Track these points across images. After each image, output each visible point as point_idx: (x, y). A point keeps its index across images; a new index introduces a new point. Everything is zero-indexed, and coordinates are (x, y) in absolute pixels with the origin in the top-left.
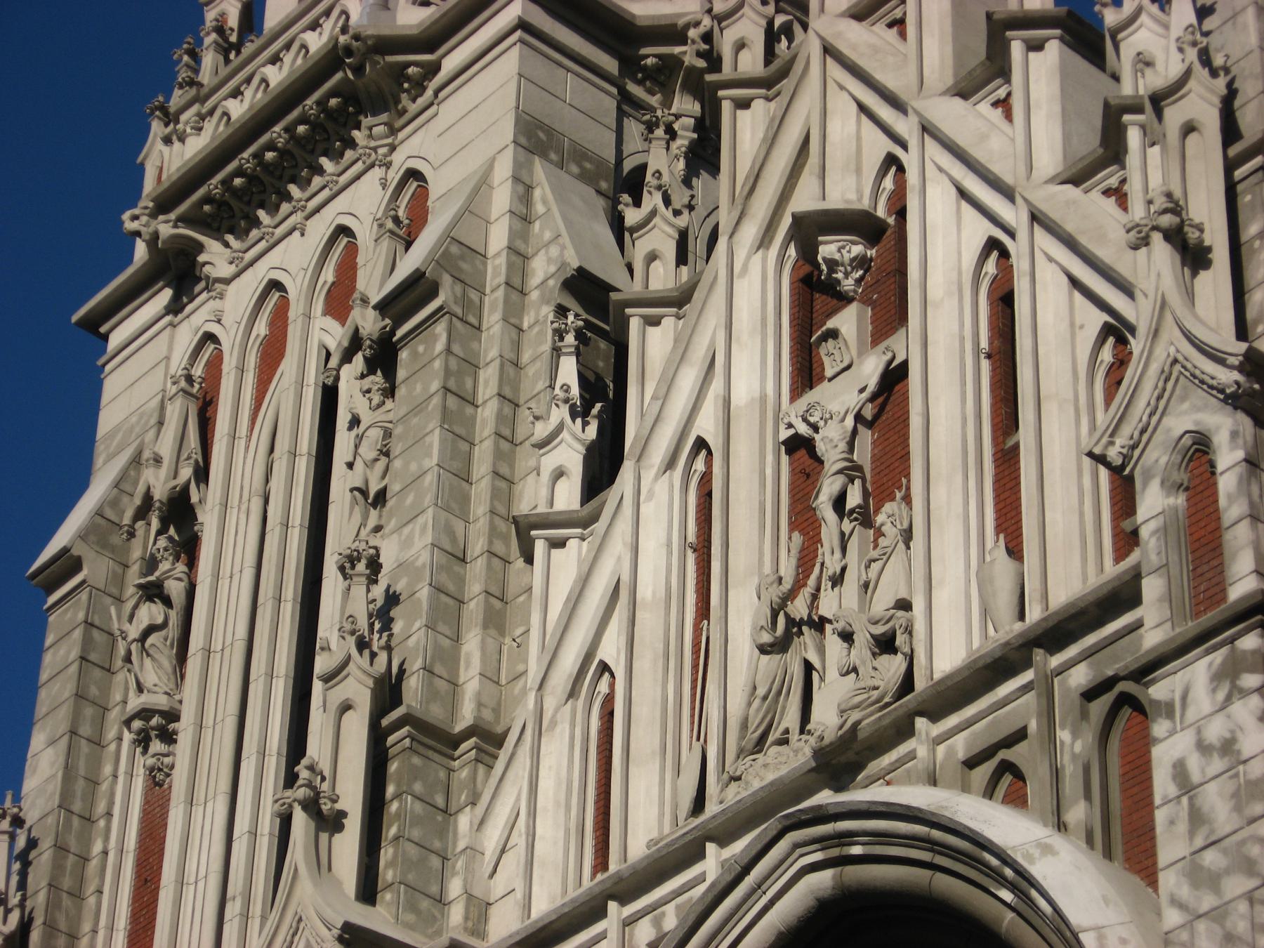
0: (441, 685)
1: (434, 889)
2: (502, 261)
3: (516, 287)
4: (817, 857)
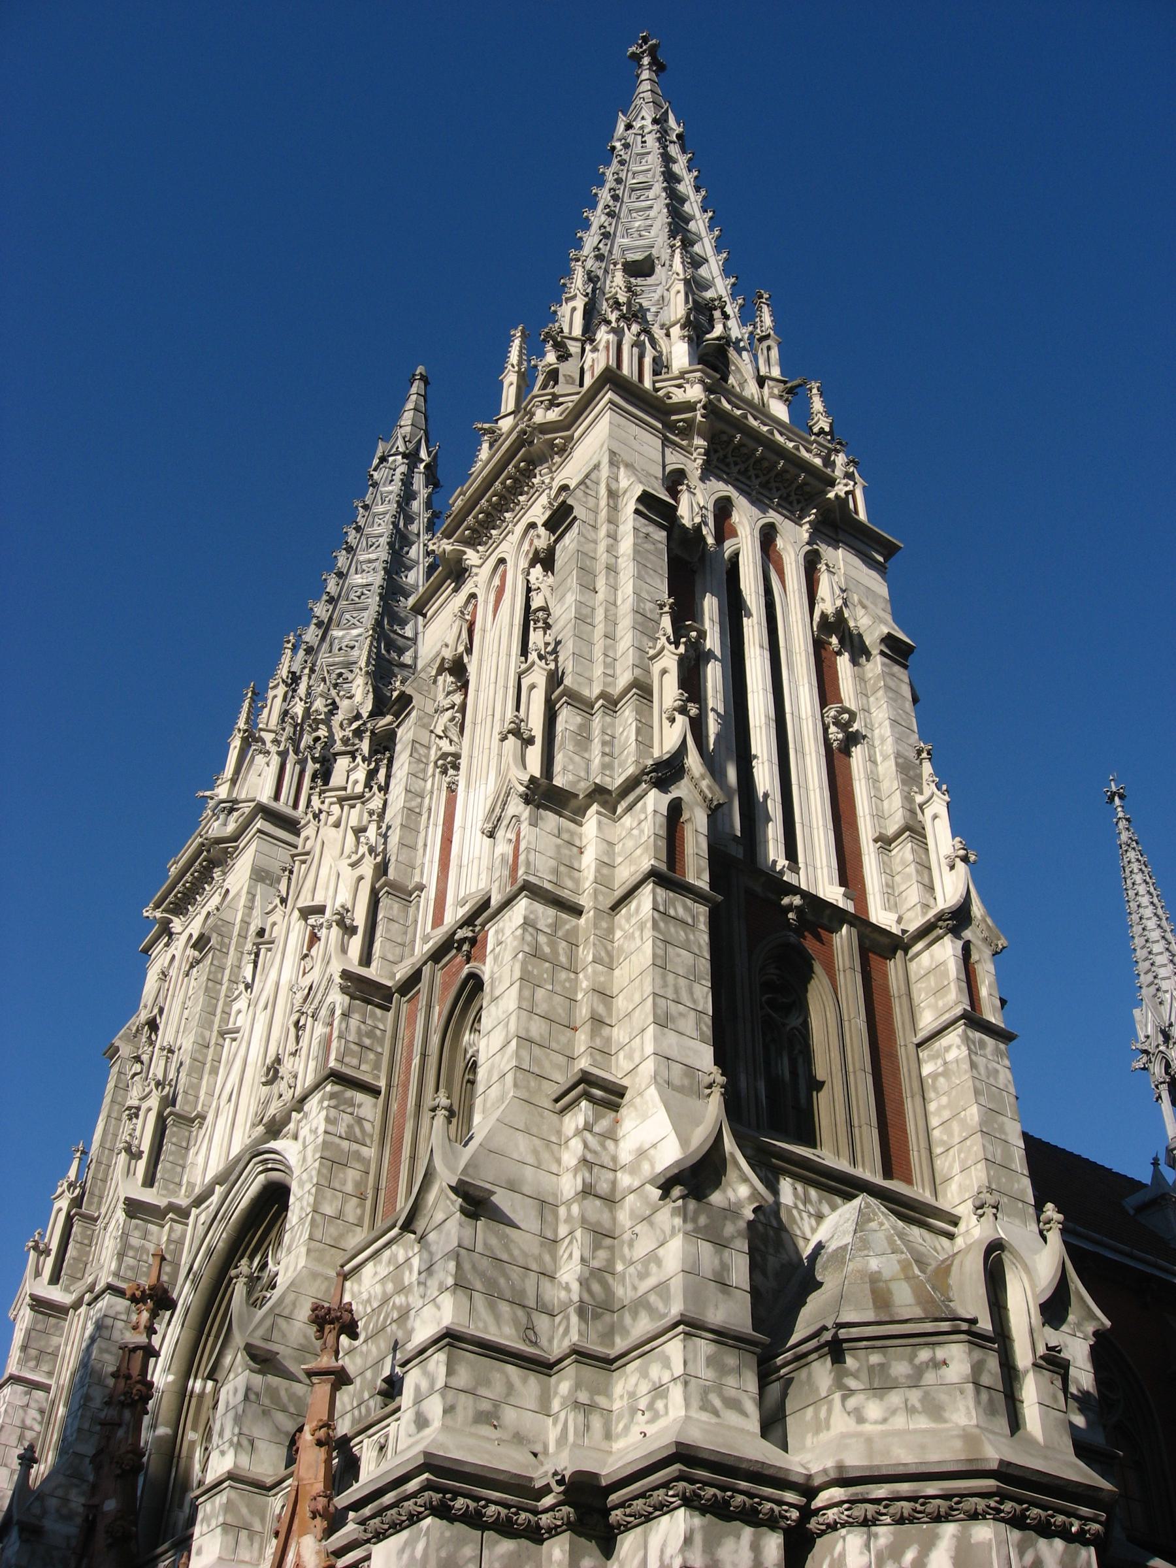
0: (191, 1098)
4: (261, 1168)
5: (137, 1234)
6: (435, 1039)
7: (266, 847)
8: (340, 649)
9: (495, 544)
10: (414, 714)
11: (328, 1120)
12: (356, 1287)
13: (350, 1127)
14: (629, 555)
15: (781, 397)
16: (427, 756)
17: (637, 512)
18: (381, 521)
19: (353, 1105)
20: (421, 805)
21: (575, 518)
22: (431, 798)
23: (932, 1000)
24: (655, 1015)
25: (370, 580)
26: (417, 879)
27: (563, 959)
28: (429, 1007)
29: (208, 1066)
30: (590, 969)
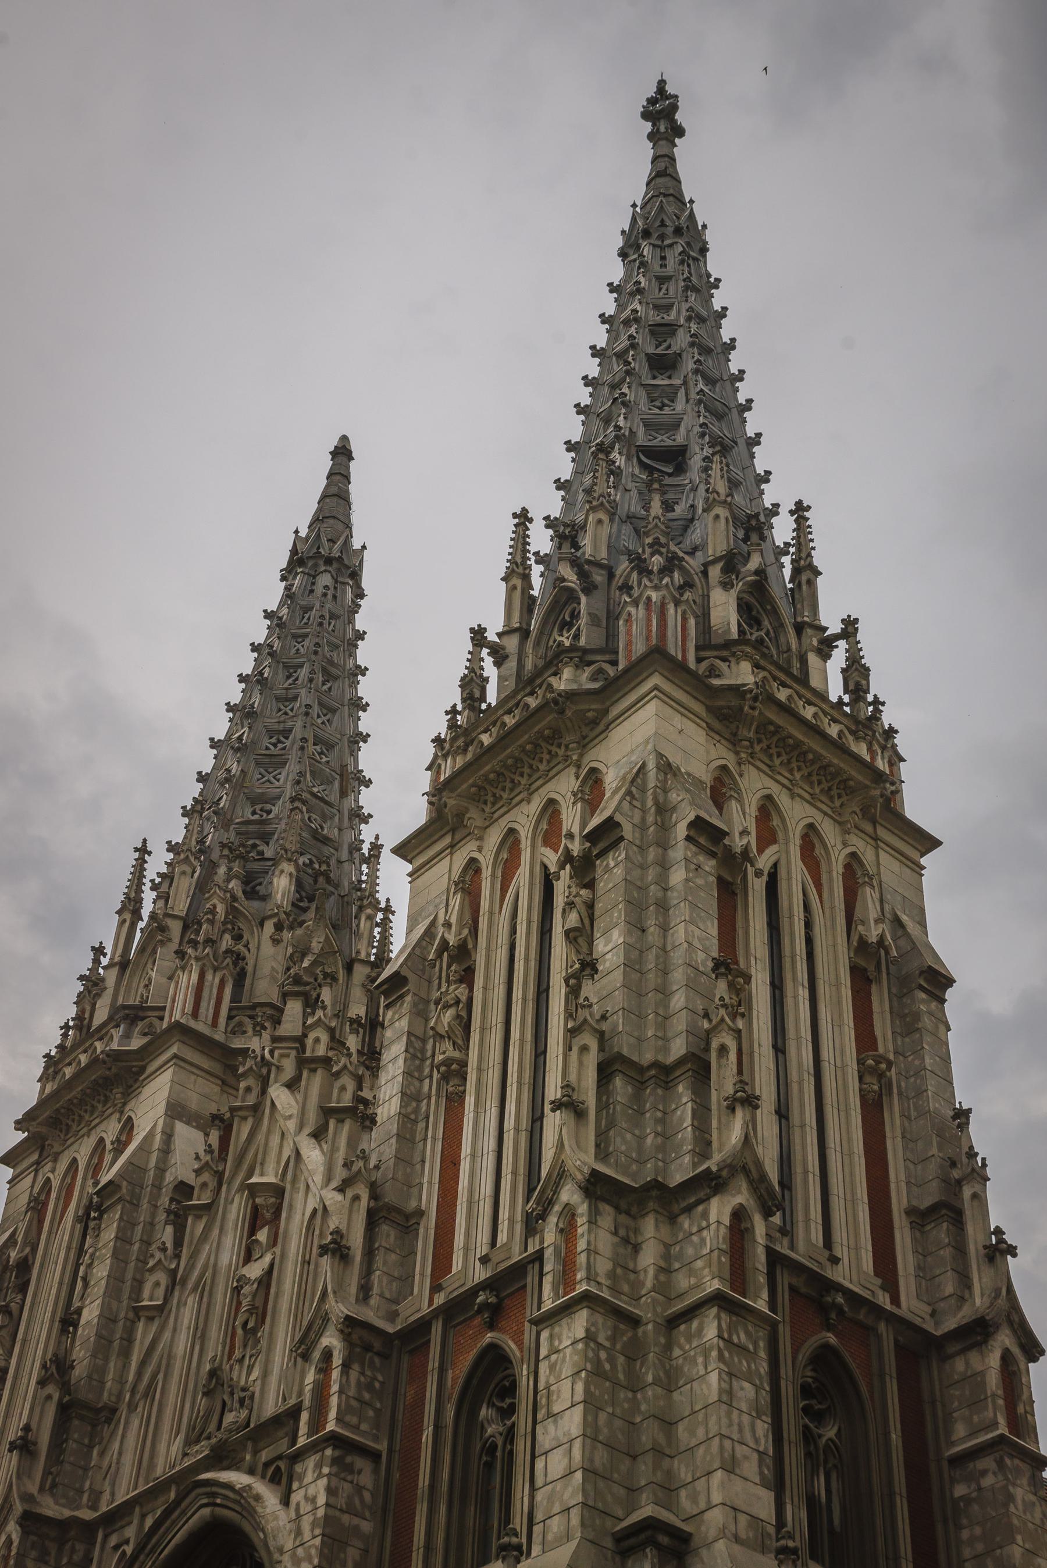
1: (77, 1486)
3: (158, 1186)
4: (205, 1501)
6: (450, 1412)
10: (408, 998)
11: (330, 1491)
16: (423, 1050)
17: (688, 838)
20: (416, 1111)
21: (622, 838)
23: (966, 1412)
24: (723, 1460)
26: (413, 1204)
27: (621, 1376)
29: (116, 1344)
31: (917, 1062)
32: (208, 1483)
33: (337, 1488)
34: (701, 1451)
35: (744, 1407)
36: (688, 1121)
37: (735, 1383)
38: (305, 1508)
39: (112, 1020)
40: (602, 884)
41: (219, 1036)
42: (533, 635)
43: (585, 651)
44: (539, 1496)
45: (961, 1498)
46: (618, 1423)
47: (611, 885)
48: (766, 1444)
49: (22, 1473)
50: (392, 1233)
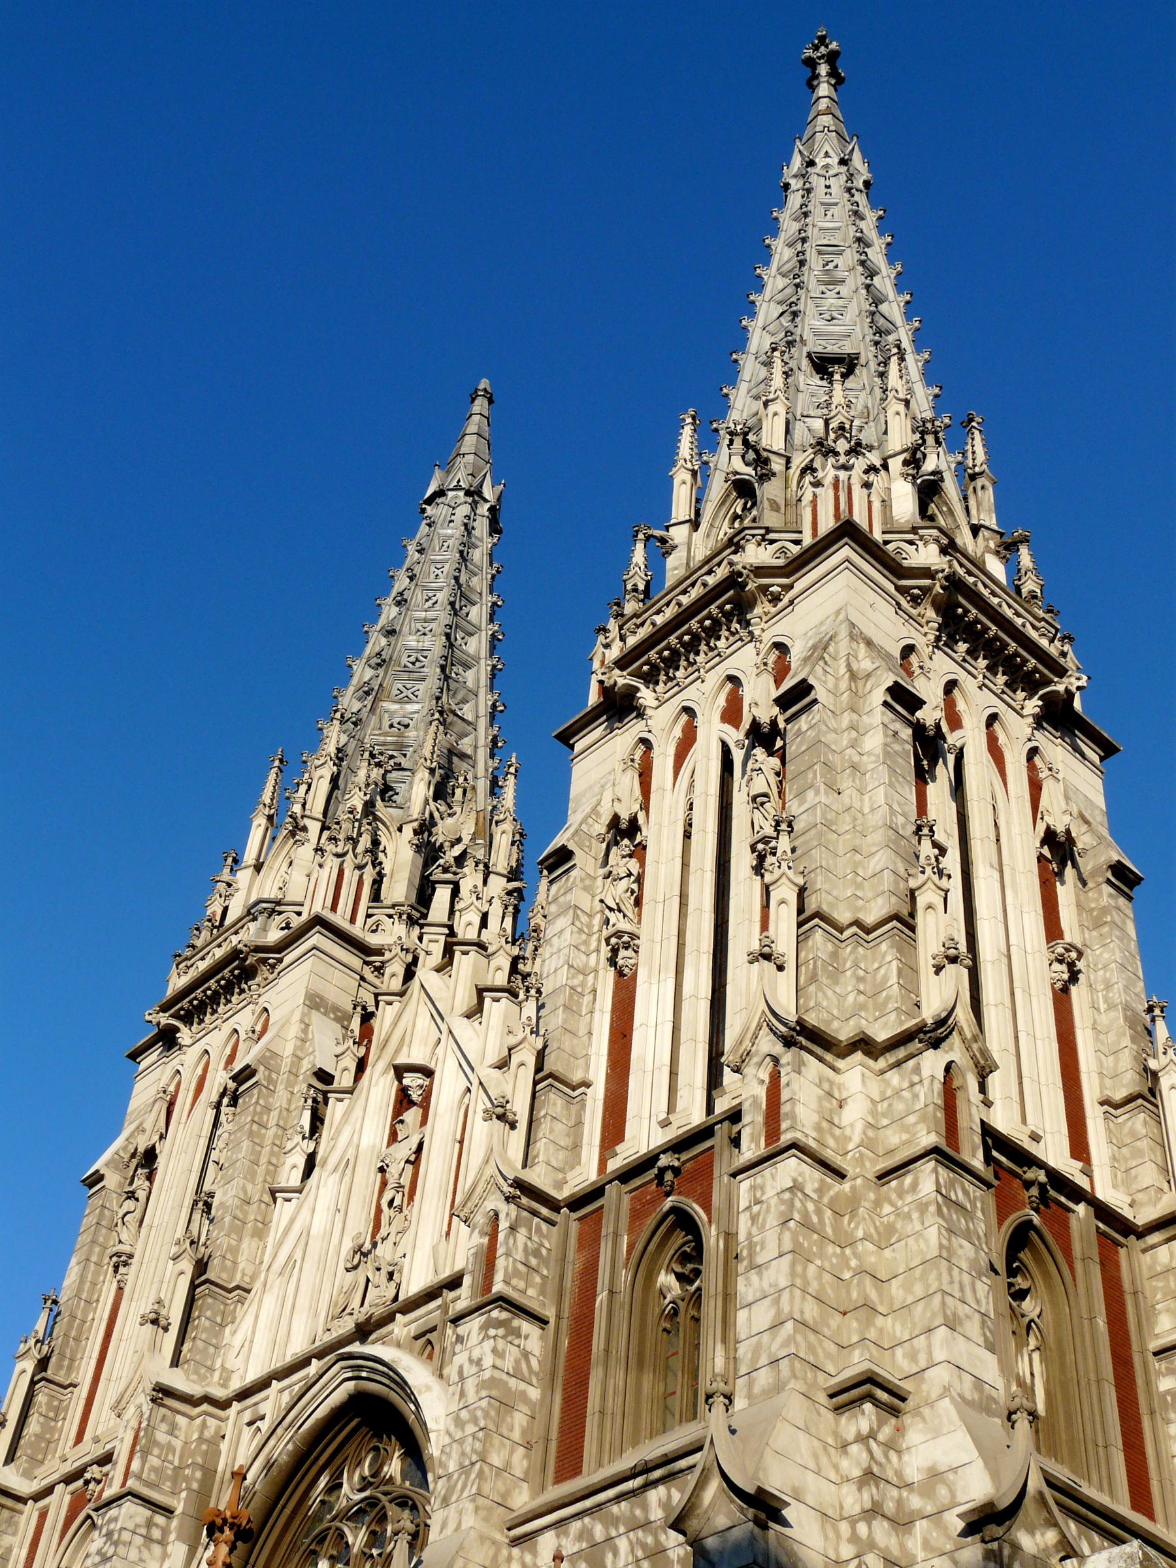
0: (229, 1263)
1: (209, 1363)
2: (289, 1060)
4: (350, 1374)
5: (164, 1427)
6: (624, 1276)
7: (322, 968)
8: (391, 726)
9: (677, 689)
10: (573, 873)
12: (528, 1558)
13: (517, 1362)
14: (878, 756)
15: (997, 553)
16: (590, 926)
18: (438, 572)
19: (519, 1336)
20: (583, 984)
21: (815, 701)
22: (596, 978)
24: (945, 1316)
25: (427, 644)
27: (829, 1230)
28: (616, 1235)
30: (860, 1247)
31: (1106, 956)
32: (351, 1356)
33: (504, 1351)
34: (920, 1307)
35: (965, 1266)
36: (894, 979)
37: (953, 1239)
38: (469, 1370)
39: (250, 914)
40: (794, 748)
41: (357, 930)
42: (703, 527)
43: (768, 530)
44: (743, 1350)
45: (1168, 1392)
46: (827, 1277)
47: (804, 748)
48: (989, 1307)
49: (154, 1347)
50: (560, 1102)
